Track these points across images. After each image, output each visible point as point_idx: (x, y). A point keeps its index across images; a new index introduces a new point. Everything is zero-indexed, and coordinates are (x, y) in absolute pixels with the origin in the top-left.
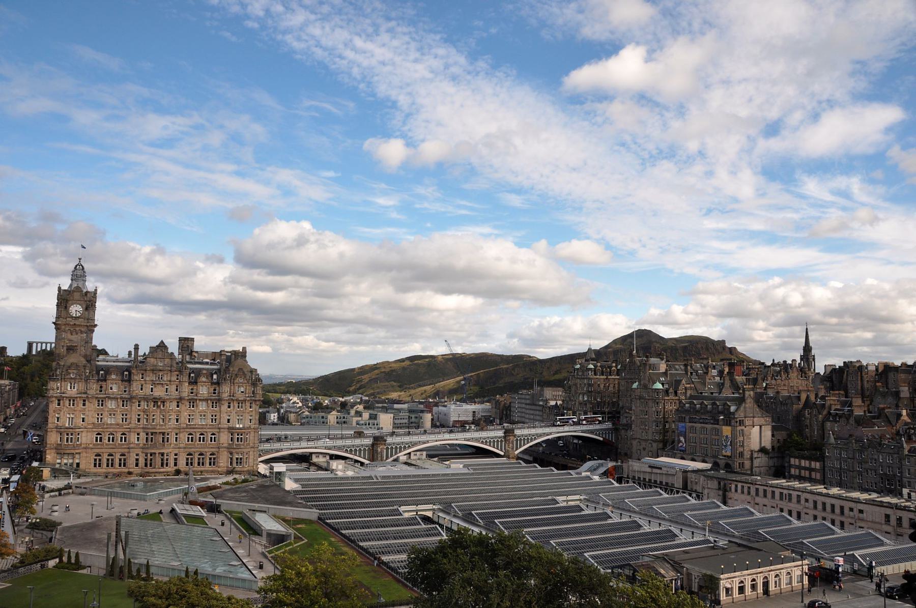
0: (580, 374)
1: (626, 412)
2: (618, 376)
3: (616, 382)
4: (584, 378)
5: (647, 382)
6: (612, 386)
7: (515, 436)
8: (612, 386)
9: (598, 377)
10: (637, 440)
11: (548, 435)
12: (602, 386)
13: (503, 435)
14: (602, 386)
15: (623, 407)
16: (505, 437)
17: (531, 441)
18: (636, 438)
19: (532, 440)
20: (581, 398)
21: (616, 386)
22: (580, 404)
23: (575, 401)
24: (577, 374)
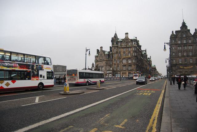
1: (180, 68)
4: (128, 47)
15: (176, 65)
22: (124, 66)
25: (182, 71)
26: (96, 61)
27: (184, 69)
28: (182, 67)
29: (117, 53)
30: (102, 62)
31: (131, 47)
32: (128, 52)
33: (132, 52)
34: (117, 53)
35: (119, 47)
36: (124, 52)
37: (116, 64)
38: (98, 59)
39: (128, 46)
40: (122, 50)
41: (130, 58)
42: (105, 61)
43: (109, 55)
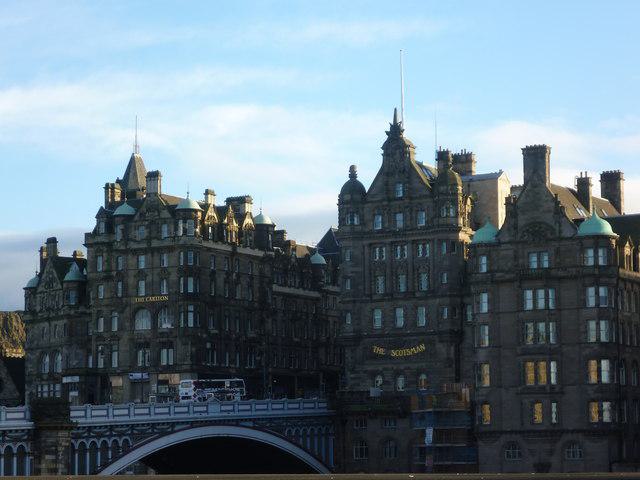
0: (141, 233)
1: (376, 357)
2: (261, 249)
3: (256, 272)
4: (160, 250)
5: (549, 218)
6: (244, 281)
7: (73, 426)
8: (244, 281)
9: (211, 244)
10: (503, 439)
11: (163, 434)
12: (221, 279)
13: (28, 425)
14: (221, 279)
15: (357, 338)
16: (34, 435)
17: (116, 458)
18: (502, 432)
19: (127, 450)
20: (143, 324)
21: (256, 285)
22: (140, 344)
23: (116, 337)
24: (126, 239)
25: (380, 368)
26: (28, 317)
27: (391, 358)
28: (381, 351)
29: (108, 278)
30: (53, 323)
31: (170, 249)
32: (156, 271)
33: (173, 277)
34: (108, 278)
35: (117, 246)
36: (141, 274)
37: (105, 335)
38: (38, 308)
39: (155, 244)
40: (132, 260)
41: (164, 306)
42: (62, 317)
43: (83, 287)
